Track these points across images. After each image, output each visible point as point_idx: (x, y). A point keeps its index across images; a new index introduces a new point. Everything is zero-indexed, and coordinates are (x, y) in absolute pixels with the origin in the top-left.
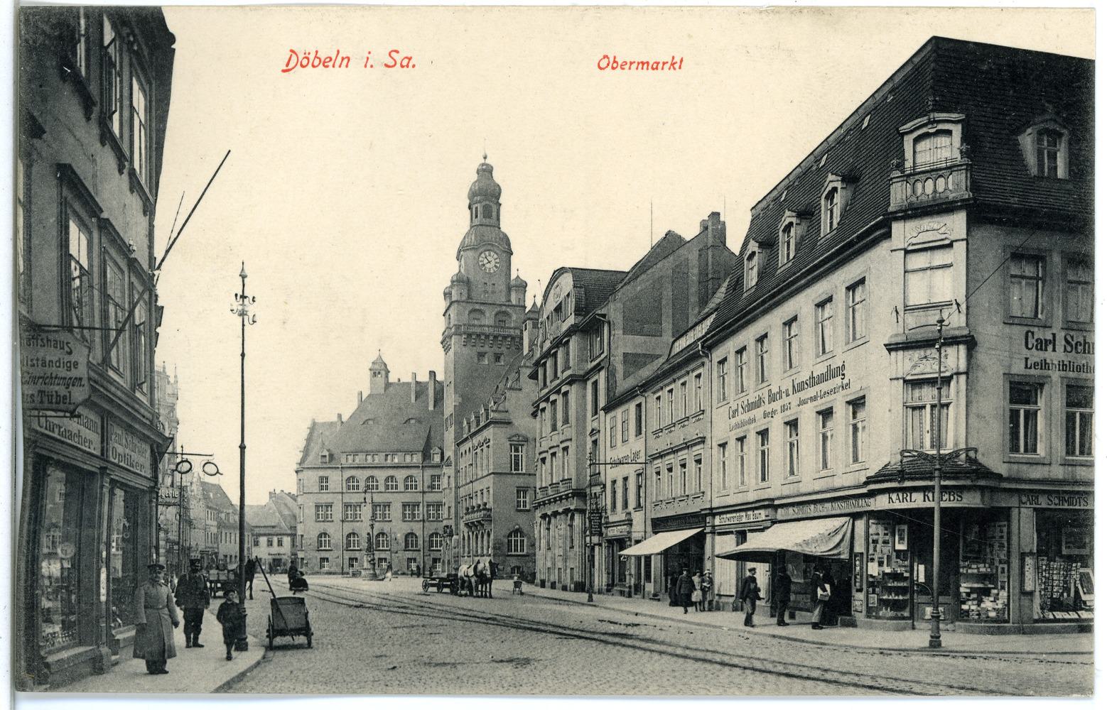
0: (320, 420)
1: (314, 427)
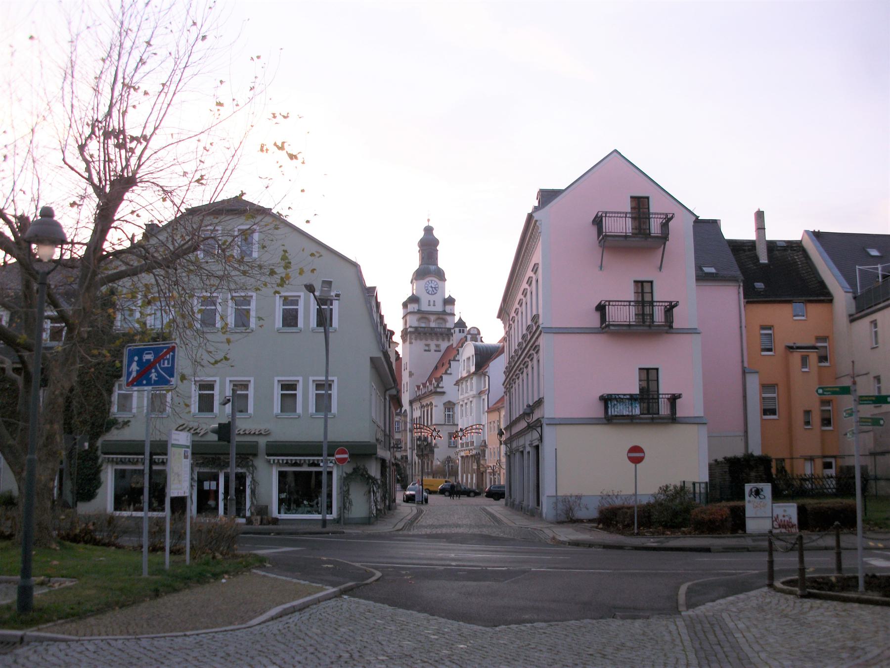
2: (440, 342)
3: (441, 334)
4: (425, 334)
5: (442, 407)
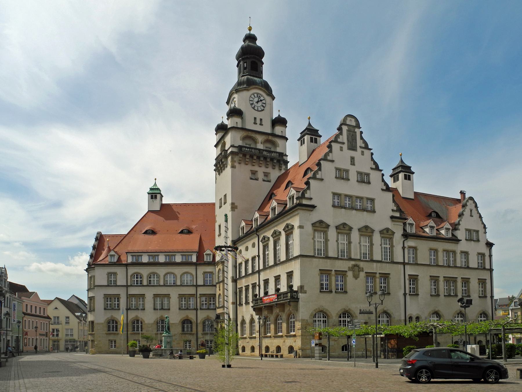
1: (100, 239)
2: (270, 170)
3: (272, 159)
4: (252, 157)
5: (309, 228)
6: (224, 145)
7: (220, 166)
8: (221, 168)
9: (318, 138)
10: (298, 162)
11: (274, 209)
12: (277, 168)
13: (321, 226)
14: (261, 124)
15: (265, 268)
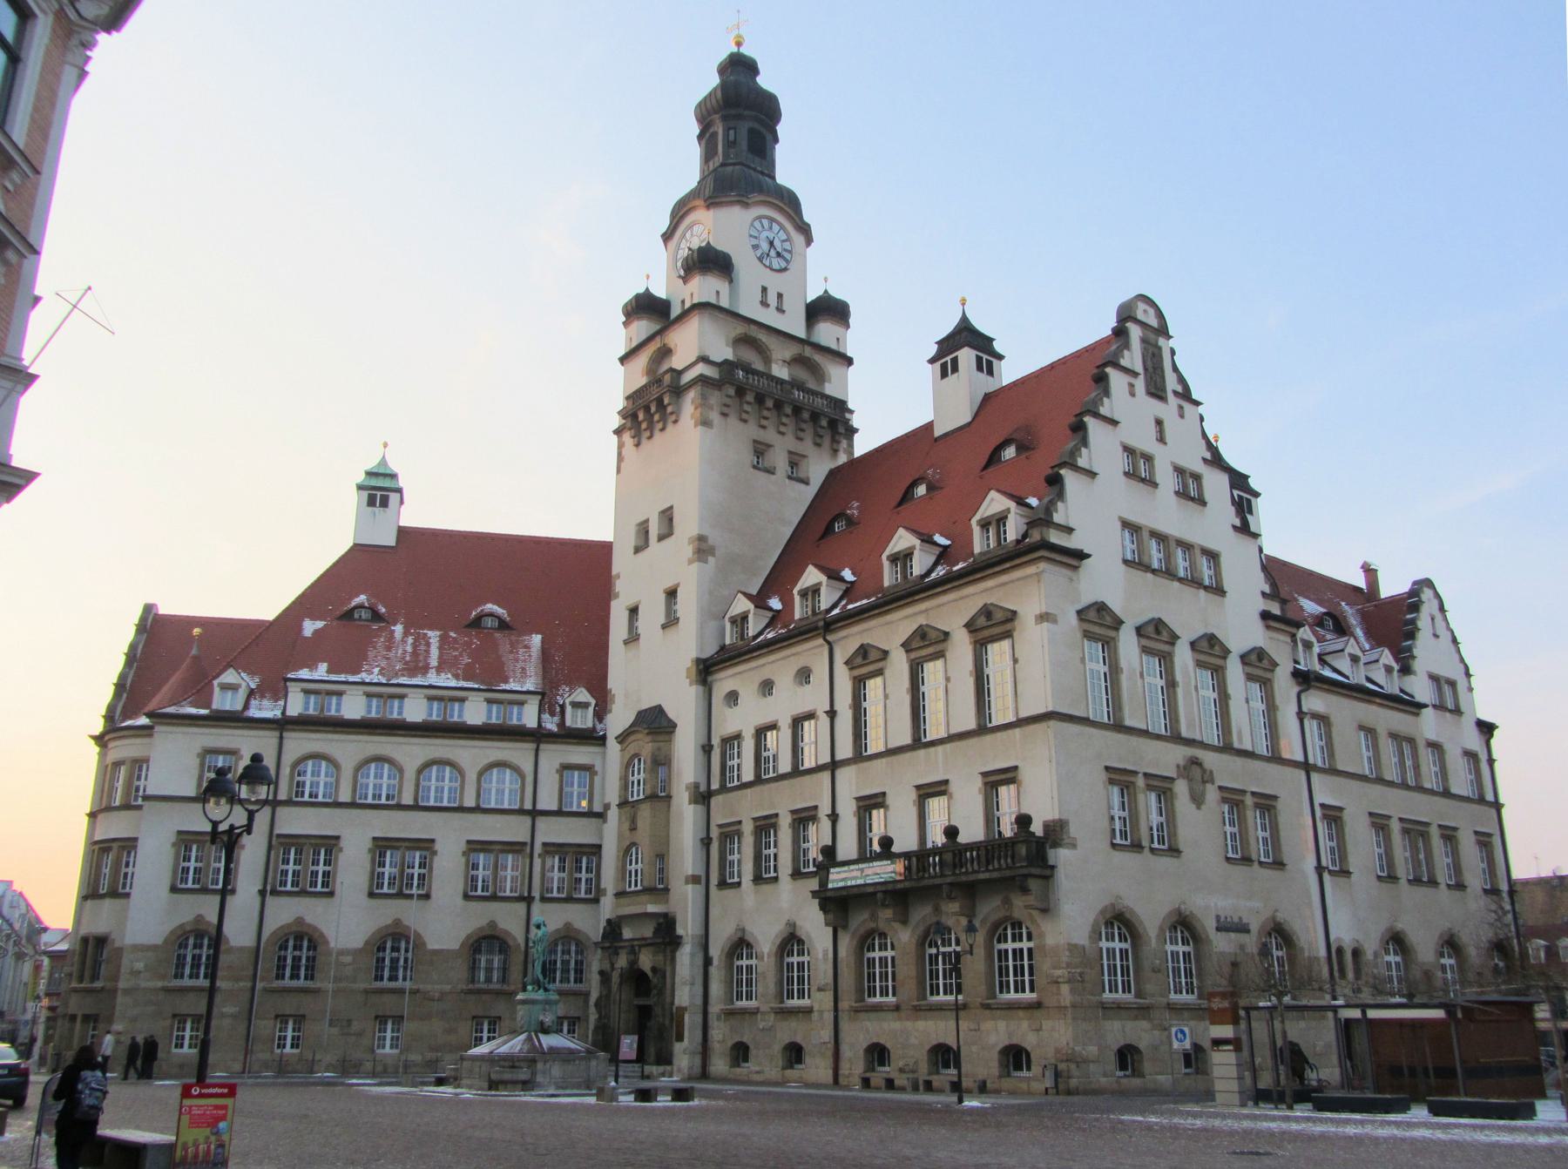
0: (168, 607)
2: (807, 447)
3: (815, 417)
4: (760, 399)
6: (666, 352)
7: (645, 413)
8: (651, 428)
9: (995, 362)
10: (929, 427)
11: (903, 558)
12: (827, 441)
13: (1099, 622)
14: (780, 310)
15: (860, 755)
